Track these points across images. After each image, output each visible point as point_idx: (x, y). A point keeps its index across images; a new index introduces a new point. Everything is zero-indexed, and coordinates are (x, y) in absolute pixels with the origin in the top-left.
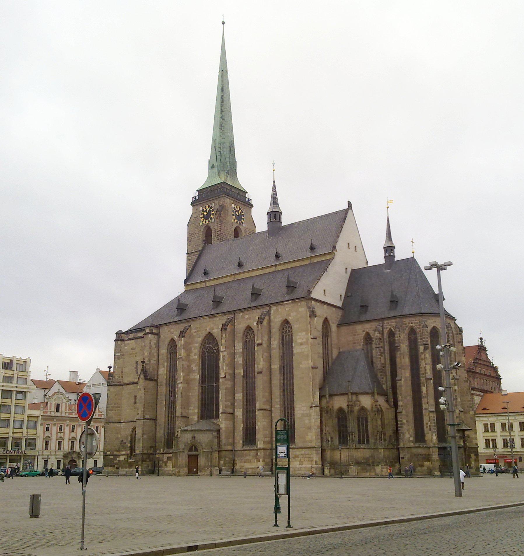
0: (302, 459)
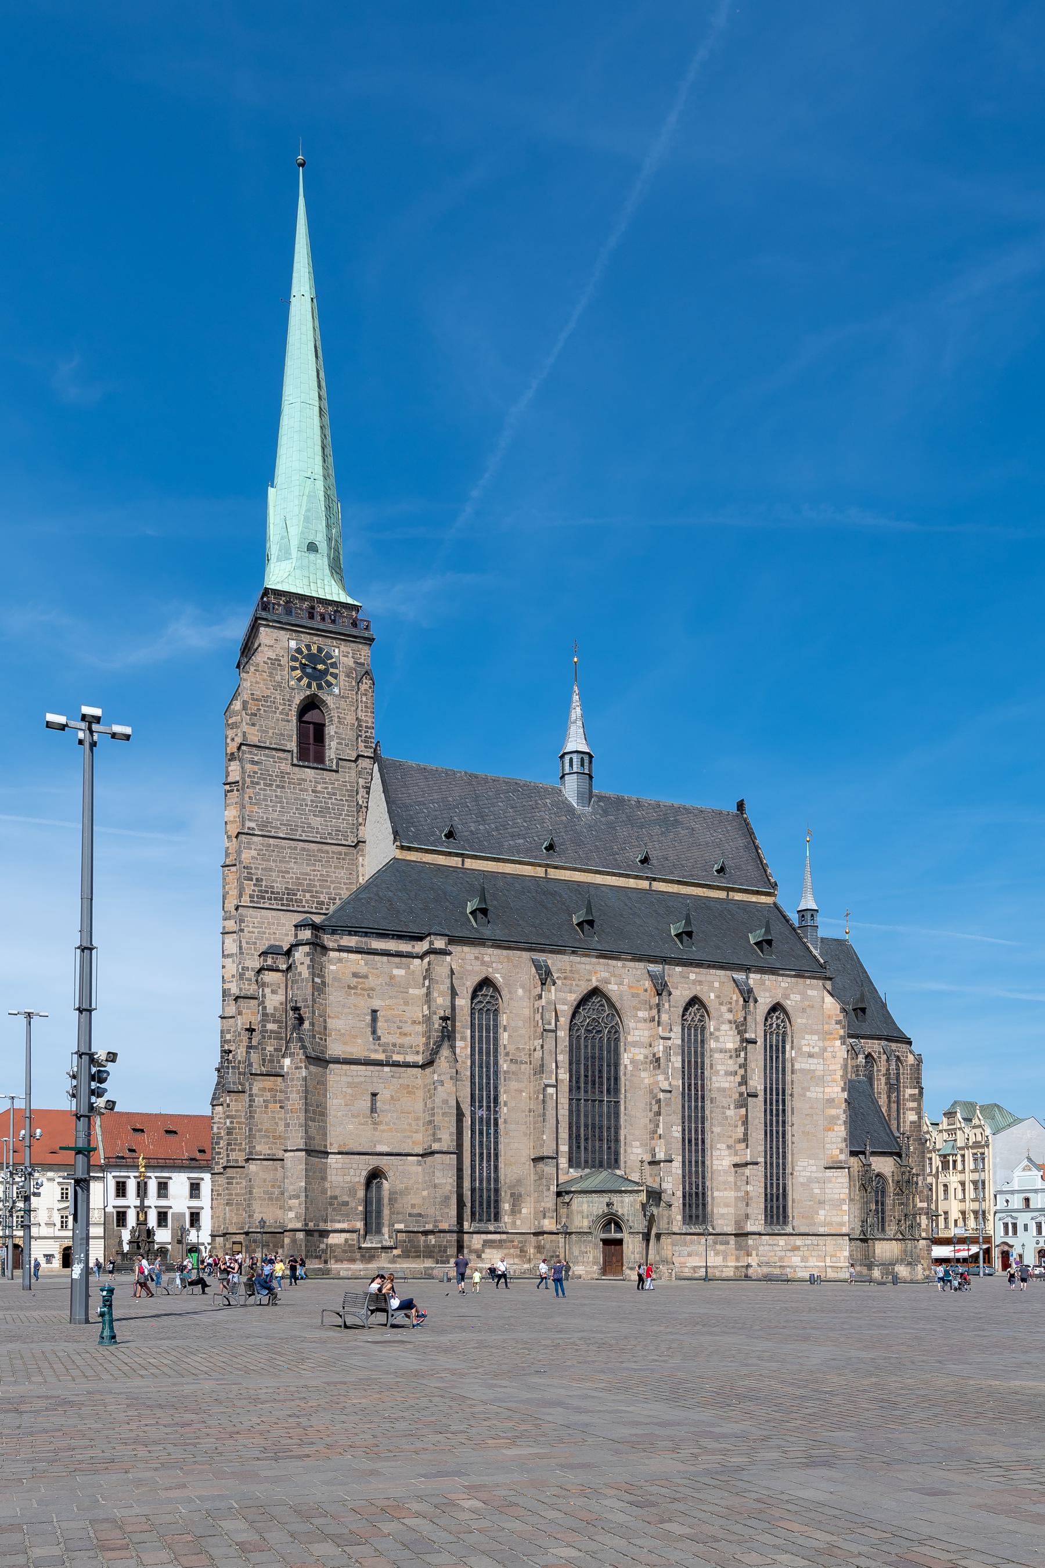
0: (806, 1253)
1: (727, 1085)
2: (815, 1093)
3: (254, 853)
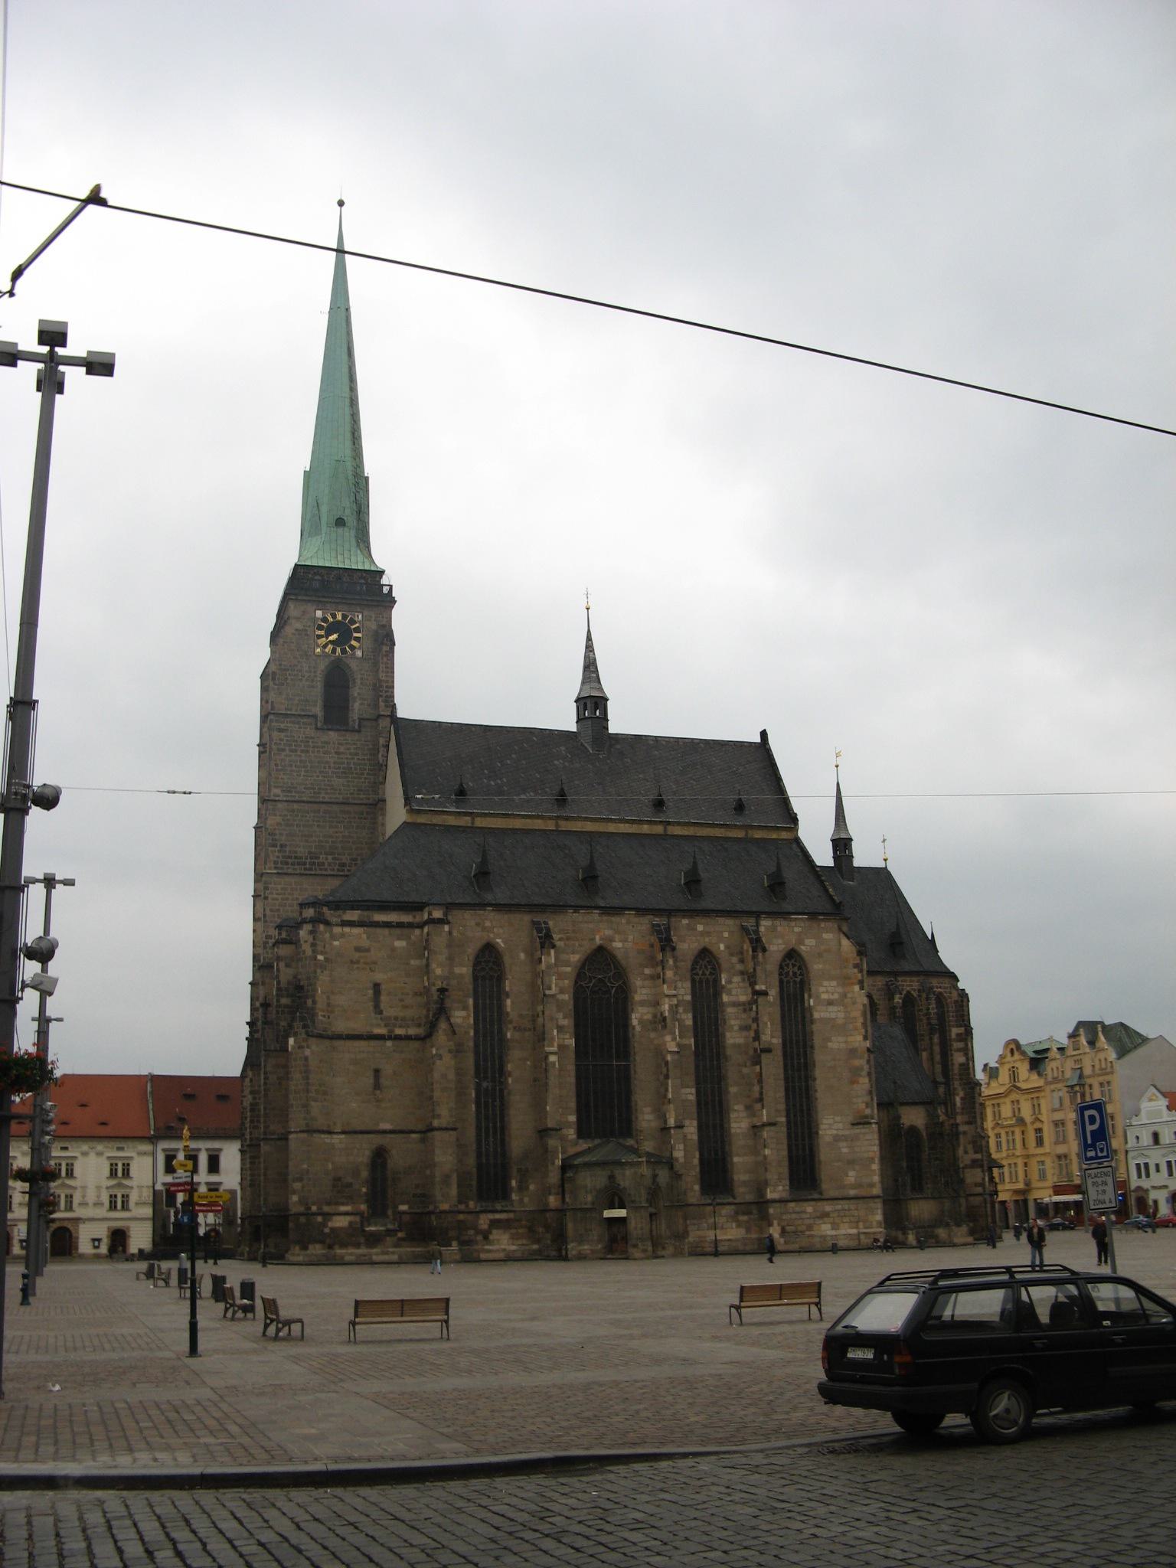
0: (837, 1220)
1: (741, 1041)
2: (837, 1043)
3: (279, 819)
